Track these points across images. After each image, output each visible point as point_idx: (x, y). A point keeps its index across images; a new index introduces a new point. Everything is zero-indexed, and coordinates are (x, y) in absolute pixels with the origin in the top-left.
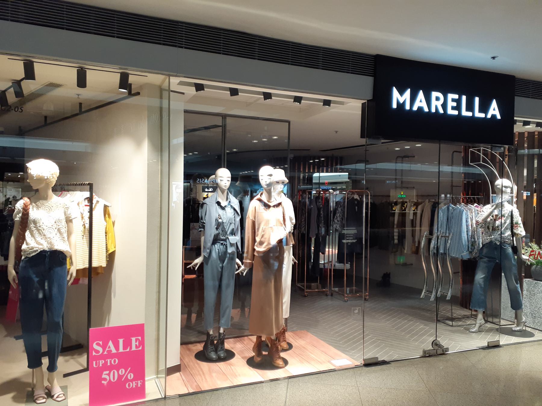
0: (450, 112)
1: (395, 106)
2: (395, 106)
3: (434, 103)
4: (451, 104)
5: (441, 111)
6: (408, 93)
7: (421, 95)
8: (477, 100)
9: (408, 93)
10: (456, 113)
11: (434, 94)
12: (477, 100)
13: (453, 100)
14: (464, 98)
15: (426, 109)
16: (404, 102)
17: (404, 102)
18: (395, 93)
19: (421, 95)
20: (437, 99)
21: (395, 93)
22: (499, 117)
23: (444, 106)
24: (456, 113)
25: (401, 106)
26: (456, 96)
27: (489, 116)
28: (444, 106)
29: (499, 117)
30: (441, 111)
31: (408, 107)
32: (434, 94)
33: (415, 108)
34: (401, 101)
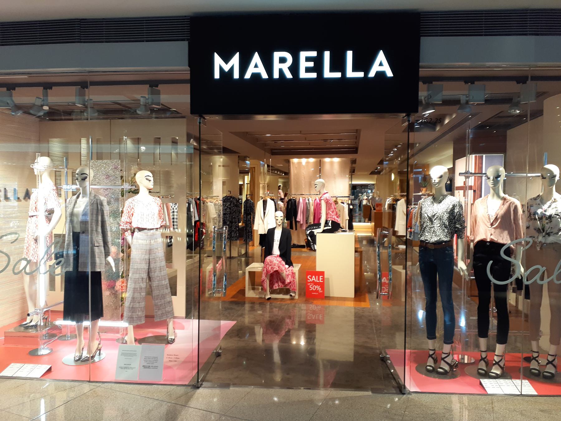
0: (303, 75)
1: (217, 75)
2: (217, 75)
3: (277, 66)
4: (303, 65)
5: (289, 75)
6: (235, 60)
7: (256, 58)
8: (350, 54)
9: (235, 60)
10: (314, 75)
11: (277, 55)
12: (350, 54)
13: (308, 59)
14: (327, 55)
15: (265, 76)
16: (232, 69)
17: (232, 69)
18: (218, 61)
19: (256, 58)
20: (283, 60)
21: (218, 61)
22: (390, 74)
23: (294, 68)
24: (314, 75)
25: (227, 75)
26: (314, 54)
27: (372, 74)
28: (294, 68)
29: (390, 74)
30: (289, 75)
31: (236, 75)
32: (277, 55)
33: (248, 76)
34: (227, 68)
